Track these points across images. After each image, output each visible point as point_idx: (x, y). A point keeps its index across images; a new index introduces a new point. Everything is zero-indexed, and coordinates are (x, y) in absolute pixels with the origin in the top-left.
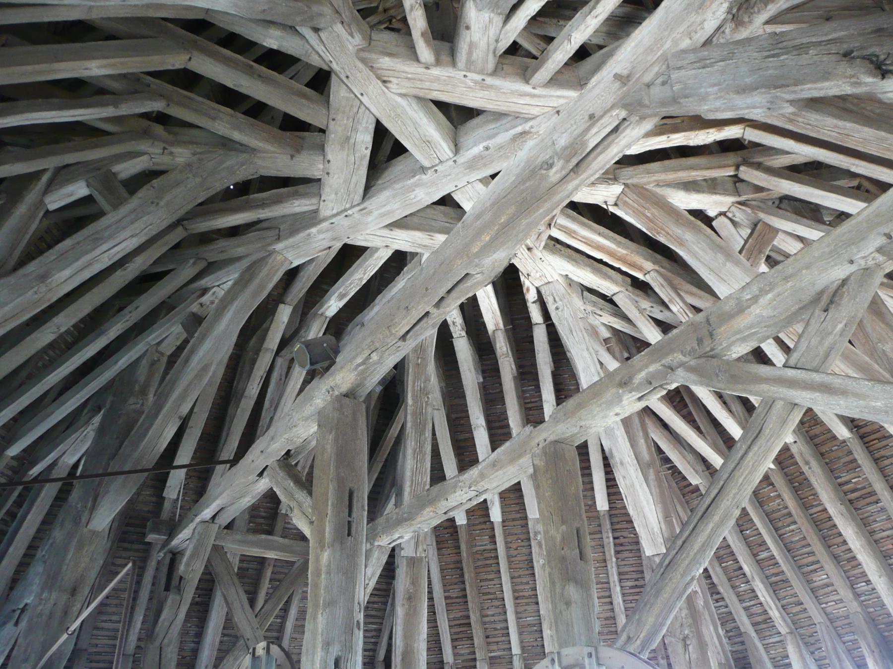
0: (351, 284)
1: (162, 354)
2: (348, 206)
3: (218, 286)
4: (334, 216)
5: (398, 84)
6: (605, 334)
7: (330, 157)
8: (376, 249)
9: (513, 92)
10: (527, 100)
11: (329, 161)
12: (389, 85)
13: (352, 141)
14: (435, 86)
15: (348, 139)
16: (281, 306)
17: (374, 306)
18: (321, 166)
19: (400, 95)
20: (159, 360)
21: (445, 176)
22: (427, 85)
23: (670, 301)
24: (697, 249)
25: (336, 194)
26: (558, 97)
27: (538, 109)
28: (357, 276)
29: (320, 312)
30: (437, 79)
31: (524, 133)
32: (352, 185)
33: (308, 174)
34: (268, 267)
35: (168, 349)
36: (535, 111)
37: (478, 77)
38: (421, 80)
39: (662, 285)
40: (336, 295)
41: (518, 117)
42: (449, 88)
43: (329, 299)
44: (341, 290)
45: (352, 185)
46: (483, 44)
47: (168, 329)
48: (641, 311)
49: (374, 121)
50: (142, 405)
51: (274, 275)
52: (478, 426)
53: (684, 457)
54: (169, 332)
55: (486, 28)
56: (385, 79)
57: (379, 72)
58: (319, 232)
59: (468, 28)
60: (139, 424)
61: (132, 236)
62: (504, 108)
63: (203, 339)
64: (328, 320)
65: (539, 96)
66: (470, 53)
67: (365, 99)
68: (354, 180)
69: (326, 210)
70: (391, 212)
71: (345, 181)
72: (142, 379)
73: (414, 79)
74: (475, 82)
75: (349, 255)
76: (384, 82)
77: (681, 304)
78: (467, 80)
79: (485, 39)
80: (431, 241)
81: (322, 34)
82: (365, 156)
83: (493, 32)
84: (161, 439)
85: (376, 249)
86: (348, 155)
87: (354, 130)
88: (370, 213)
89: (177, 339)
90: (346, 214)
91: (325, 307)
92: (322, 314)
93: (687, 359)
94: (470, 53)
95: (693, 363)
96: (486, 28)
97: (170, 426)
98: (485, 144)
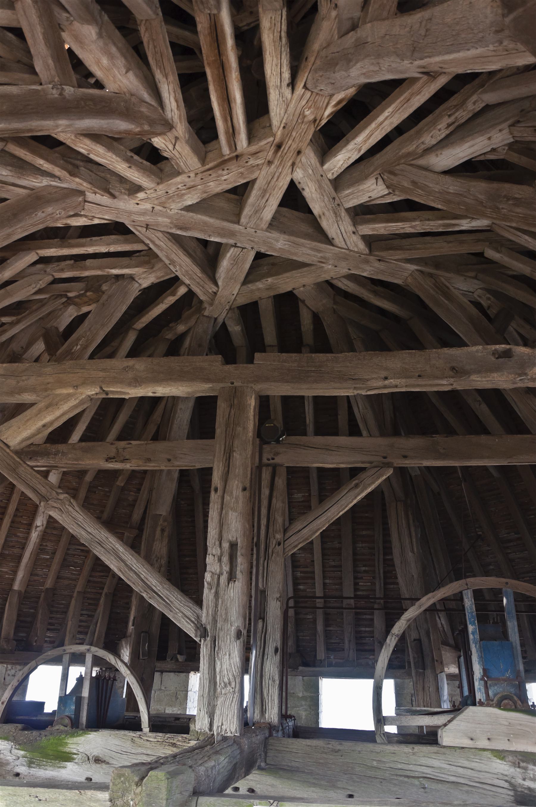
5: (211, 289)
9: (162, 250)
10: (158, 242)
12: (215, 291)
16: (486, 255)
26: (140, 232)
27: (157, 235)
30: (191, 278)
31: (181, 229)
36: (160, 235)
37: (171, 267)
38: (198, 283)
42: (190, 272)
62: (175, 247)
67: (235, 292)
70: (312, 249)
73: (201, 286)
74: (175, 266)
79: (150, 275)
80: (327, 213)
96: (144, 278)
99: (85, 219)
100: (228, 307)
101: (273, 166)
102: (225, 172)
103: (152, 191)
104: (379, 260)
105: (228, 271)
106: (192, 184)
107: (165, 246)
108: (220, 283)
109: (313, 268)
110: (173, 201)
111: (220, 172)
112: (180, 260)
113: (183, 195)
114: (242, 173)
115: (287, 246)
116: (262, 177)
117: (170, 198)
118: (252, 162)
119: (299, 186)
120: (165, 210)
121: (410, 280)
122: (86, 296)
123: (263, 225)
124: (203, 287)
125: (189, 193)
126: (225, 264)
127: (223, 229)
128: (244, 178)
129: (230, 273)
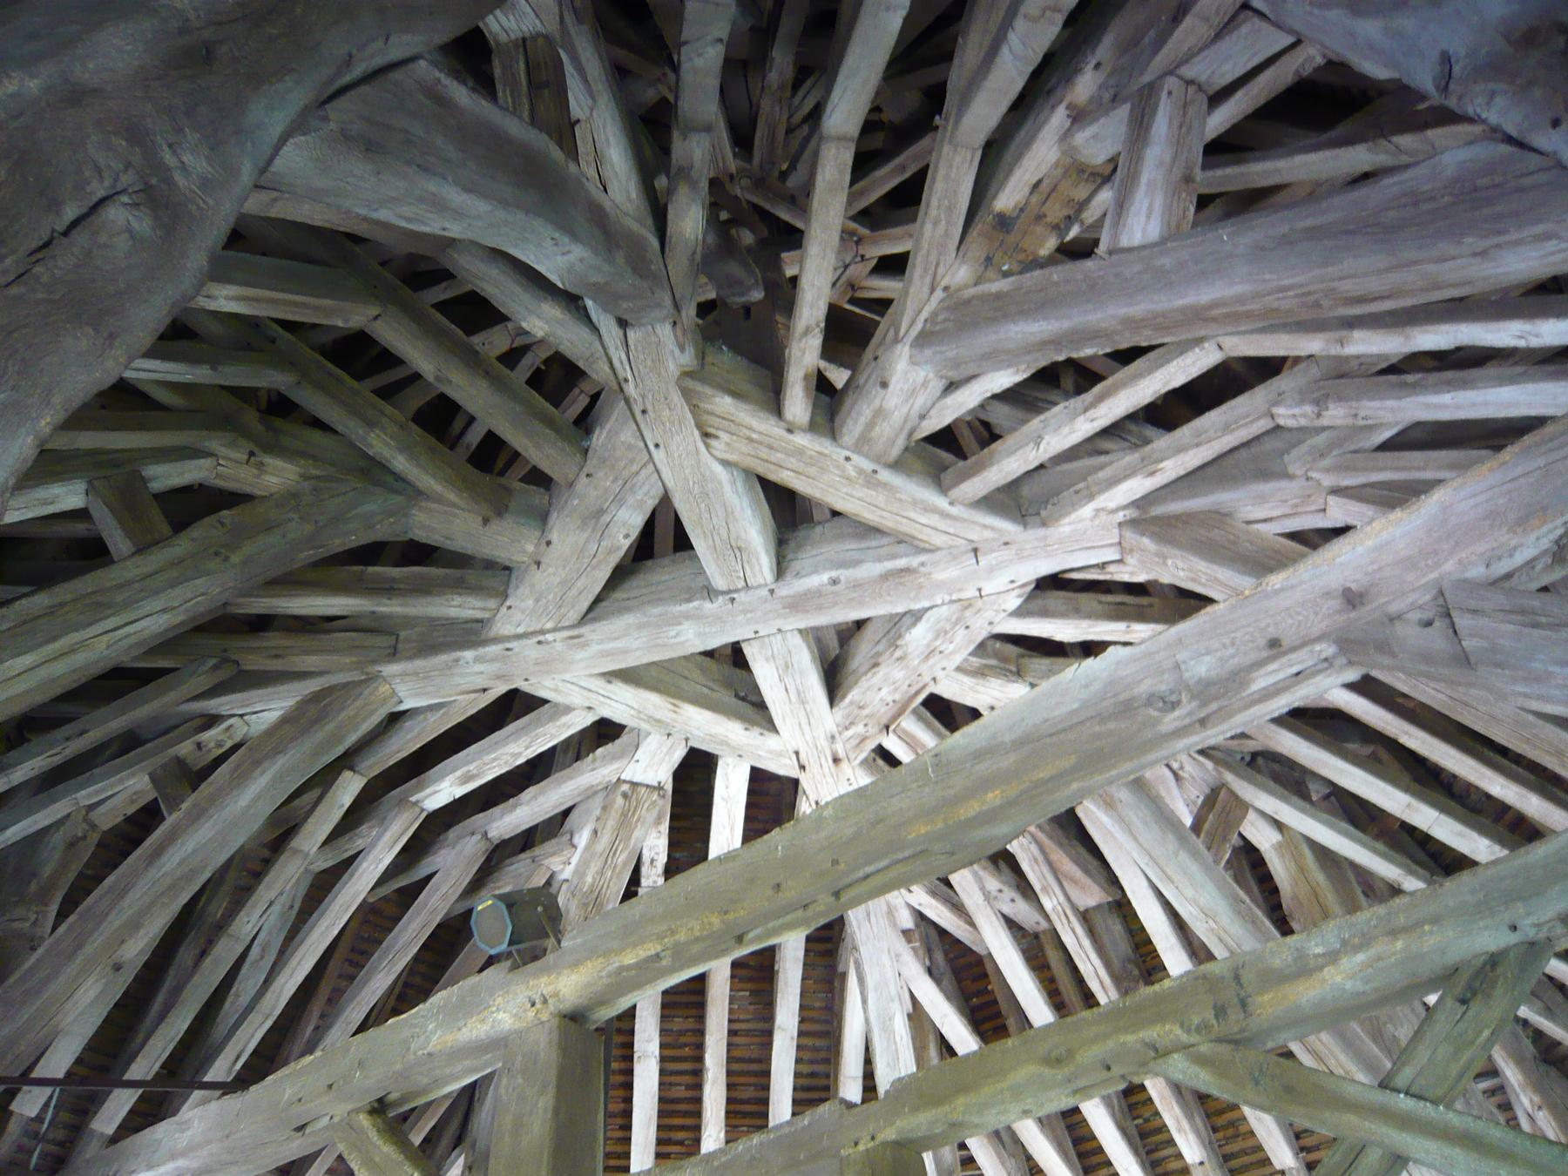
0: (495, 759)
1: (94, 827)
2: (549, 625)
3: (241, 716)
4: (518, 637)
5: (727, 444)
6: (907, 921)
7: (554, 536)
8: (568, 709)
9: (915, 503)
10: (934, 520)
11: (549, 543)
12: (713, 442)
13: (606, 518)
14: (792, 462)
15: (601, 512)
16: (347, 774)
17: (515, 807)
18: (530, 548)
19: (726, 463)
20: (84, 838)
21: (744, 612)
22: (778, 457)
23: (1044, 889)
24: (1135, 819)
25: (537, 601)
26: (985, 526)
27: (945, 538)
28: (513, 748)
29: (413, 799)
30: (800, 452)
31: (907, 571)
32: (574, 592)
33: (502, 555)
34: (358, 703)
35: (108, 818)
36: (938, 540)
37: (867, 465)
38: (771, 447)
39: (1036, 860)
40: (458, 773)
41: (904, 541)
42: (813, 471)
43: (442, 777)
44: (471, 767)
45: (574, 592)
46: (897, 418)
47: (121, 781)
48: (987, 896)
49: (661, 491)
50: (34, 923)
51: (364, 720)
52: (646, 1056)
53: (1003, 1164)
54: (125, 788)
55: (913, 392)
56: (711, 430)
57: (705, 417)
58: (477, 660)
59: (884, 385)
60: (27, 965)
61: (164, 611)
63: (198, 817)
64: (424, 815)
65: (955, 518)
66: (871, 425)
67: (658, 455)
68: (579, 584)
69: (503, 627)
70: (625, 652)
71: (563, 583)
72: (47, 871)
73: (761, 443)
74: (861, 472)
75: (514, 706)
76: (706, 435)
77: (1062, 898)
78: (848, 466)
79: (905, 410)
81: (631, 334)
82: (619, 548)
83: (920, 402)
84: (68, 1006)
85: (568, 709)
86: (587, 541)
87: (619, 500)
88: (586, 645)
89: (132, 802)
90: (541, 638)
91: (428, 791)
92: (416, 803)
93: (1194, 1039)
94: (871, 425)
95: (1205, 1048)
96: (913, 392)
97: (91, 980)
98: (834, 574)
99: (1112, 505)
100: (630, 389)
101: (822, 736)
102: (890, 699)
103: (996, 620)
104: (485, 690)
105: (729, 516)
106: (931, 661)
107: (913, 515)
108: (718, 469)
109: (574, 615)
110: (948, 620)
111: (897, 697)
112: (859, 495)
113: (936, 638)
114: (861, 708)
115: (673, 633)
116: (826, 718)
117: (956, 623)
118: (859, 729)
119: (756, 731)
120: (954, 597)
121: (384, 689)
122: (1056, 227)
123: (755, 650)
124: (751, 440)
125: (928, 645)
126: (752, 527)
127: (820, 608)
128: (851, 703)
129: (721, 513)
